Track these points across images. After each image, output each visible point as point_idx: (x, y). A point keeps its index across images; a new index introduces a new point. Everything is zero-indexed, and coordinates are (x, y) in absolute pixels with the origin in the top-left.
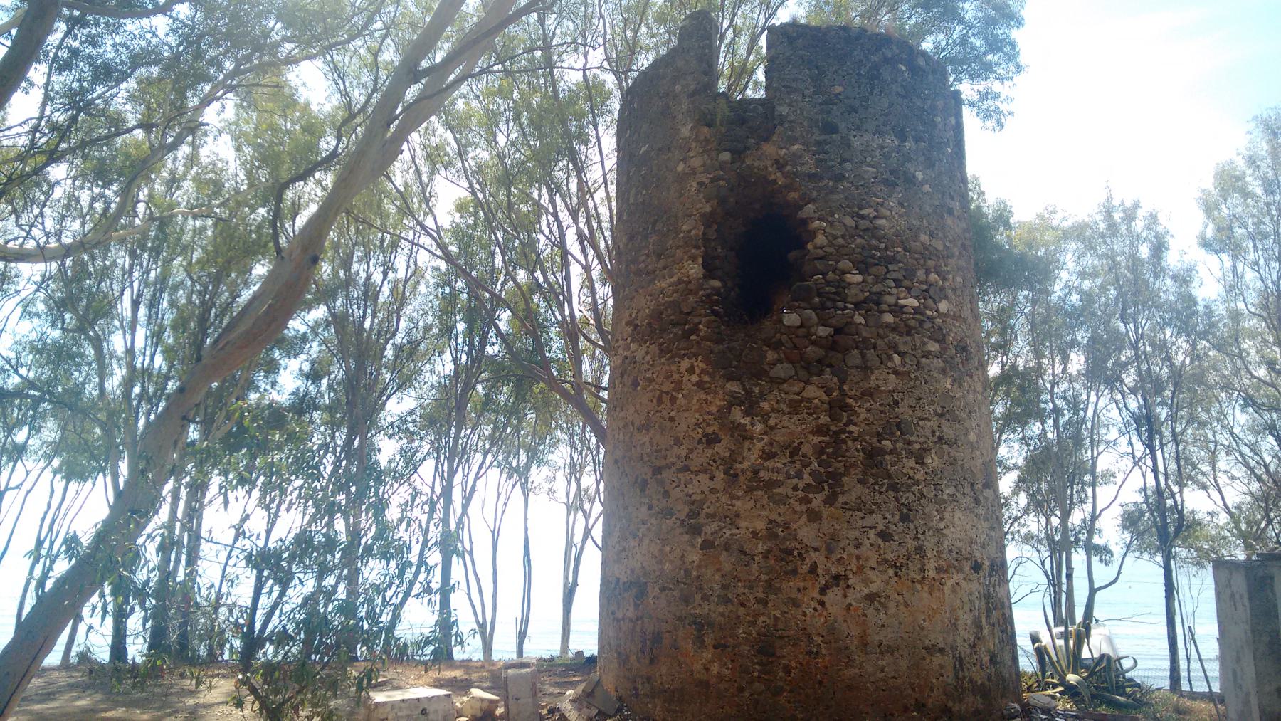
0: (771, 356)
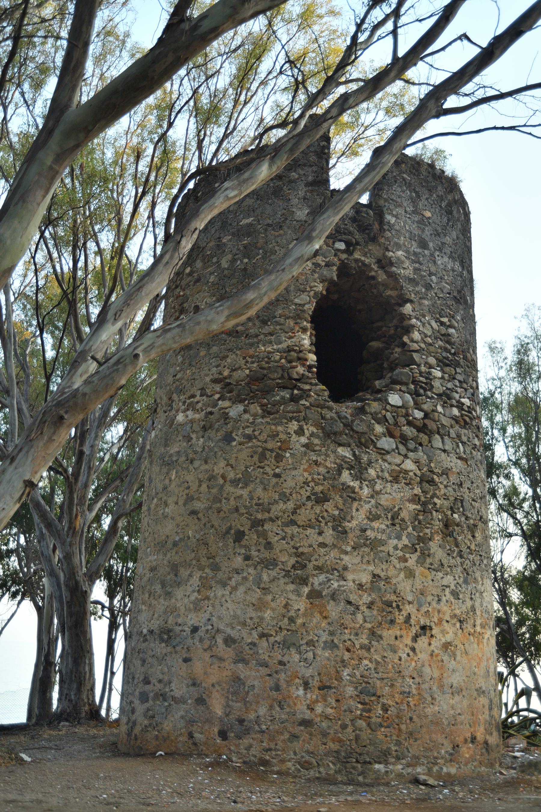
0: (379, 429)
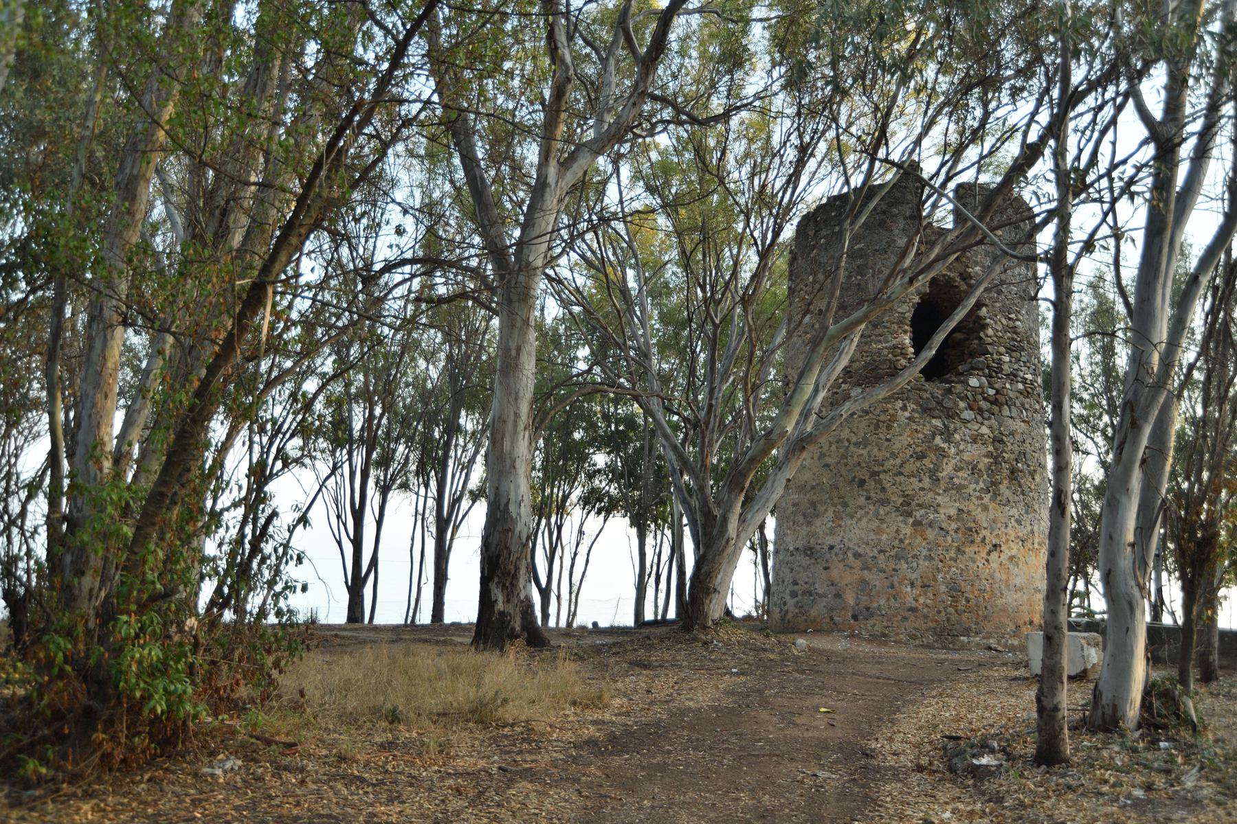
0: (962, 405)
